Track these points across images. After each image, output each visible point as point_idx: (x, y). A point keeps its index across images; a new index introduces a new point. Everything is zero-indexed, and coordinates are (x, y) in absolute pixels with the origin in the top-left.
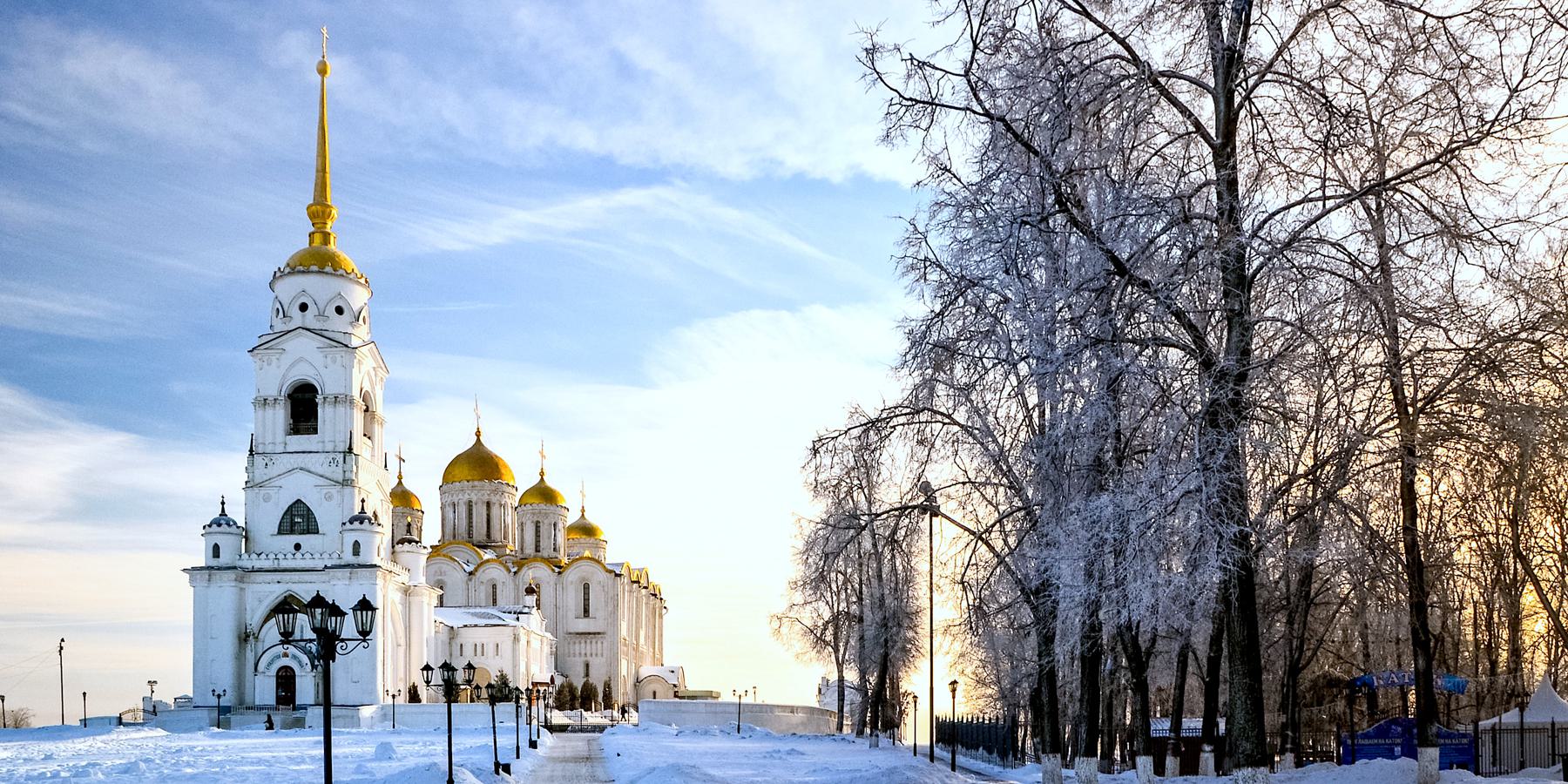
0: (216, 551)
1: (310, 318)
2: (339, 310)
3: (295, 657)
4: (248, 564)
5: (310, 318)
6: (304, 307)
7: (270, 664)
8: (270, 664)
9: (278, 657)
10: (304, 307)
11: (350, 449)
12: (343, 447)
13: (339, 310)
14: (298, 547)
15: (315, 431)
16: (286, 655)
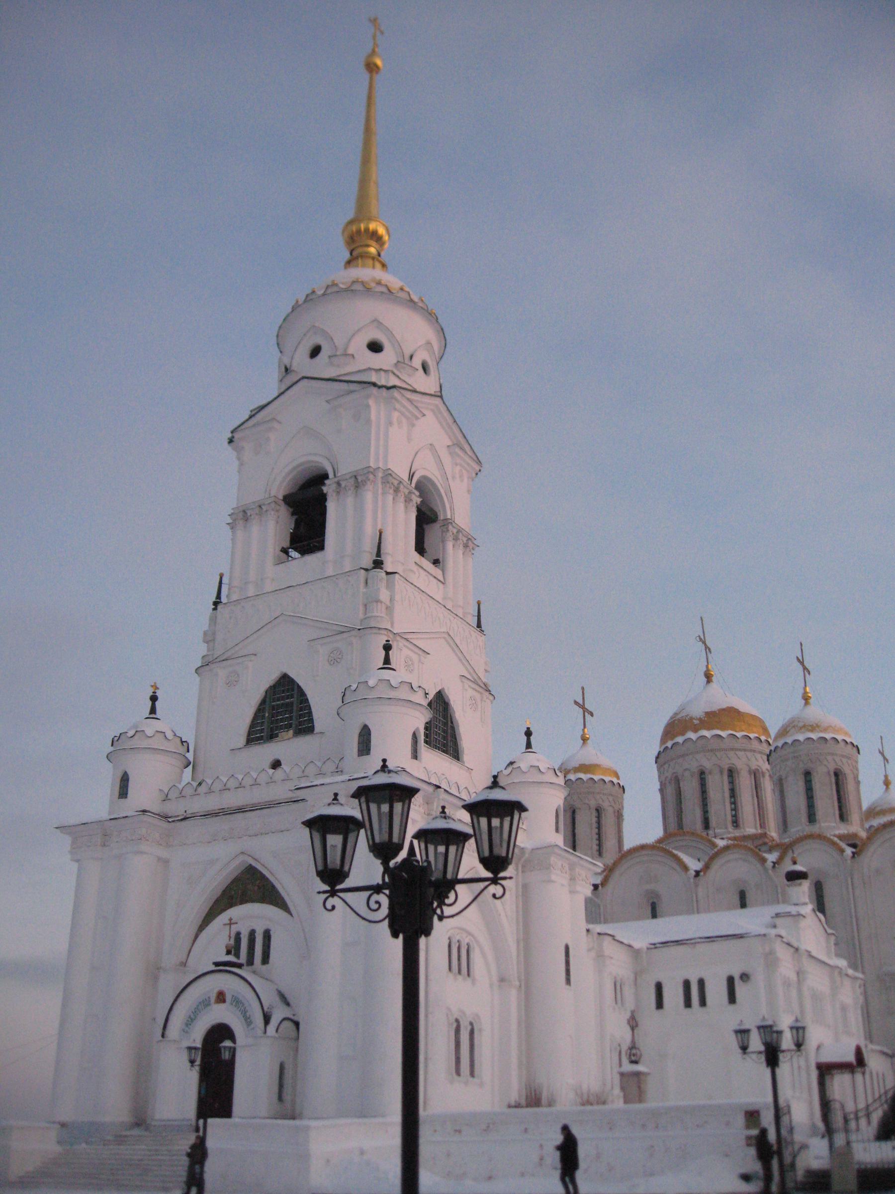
0: (124, 787)
1: (322, 367)
2: (375, 347)
3: (237, 1002)
4: (177, 808)
5: (322, 367)
6: (315, 352)
7: (190, 1021)
8: (190, 1021)
9: (205, 1004)
10: (315, 352)
11: (378, 564)
12: (367, 562)
13: (375, 347)
14: (276, 765)
15: (321, 547)
16: (221, 997)
